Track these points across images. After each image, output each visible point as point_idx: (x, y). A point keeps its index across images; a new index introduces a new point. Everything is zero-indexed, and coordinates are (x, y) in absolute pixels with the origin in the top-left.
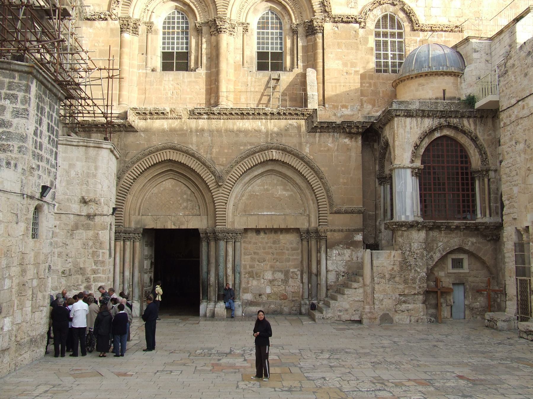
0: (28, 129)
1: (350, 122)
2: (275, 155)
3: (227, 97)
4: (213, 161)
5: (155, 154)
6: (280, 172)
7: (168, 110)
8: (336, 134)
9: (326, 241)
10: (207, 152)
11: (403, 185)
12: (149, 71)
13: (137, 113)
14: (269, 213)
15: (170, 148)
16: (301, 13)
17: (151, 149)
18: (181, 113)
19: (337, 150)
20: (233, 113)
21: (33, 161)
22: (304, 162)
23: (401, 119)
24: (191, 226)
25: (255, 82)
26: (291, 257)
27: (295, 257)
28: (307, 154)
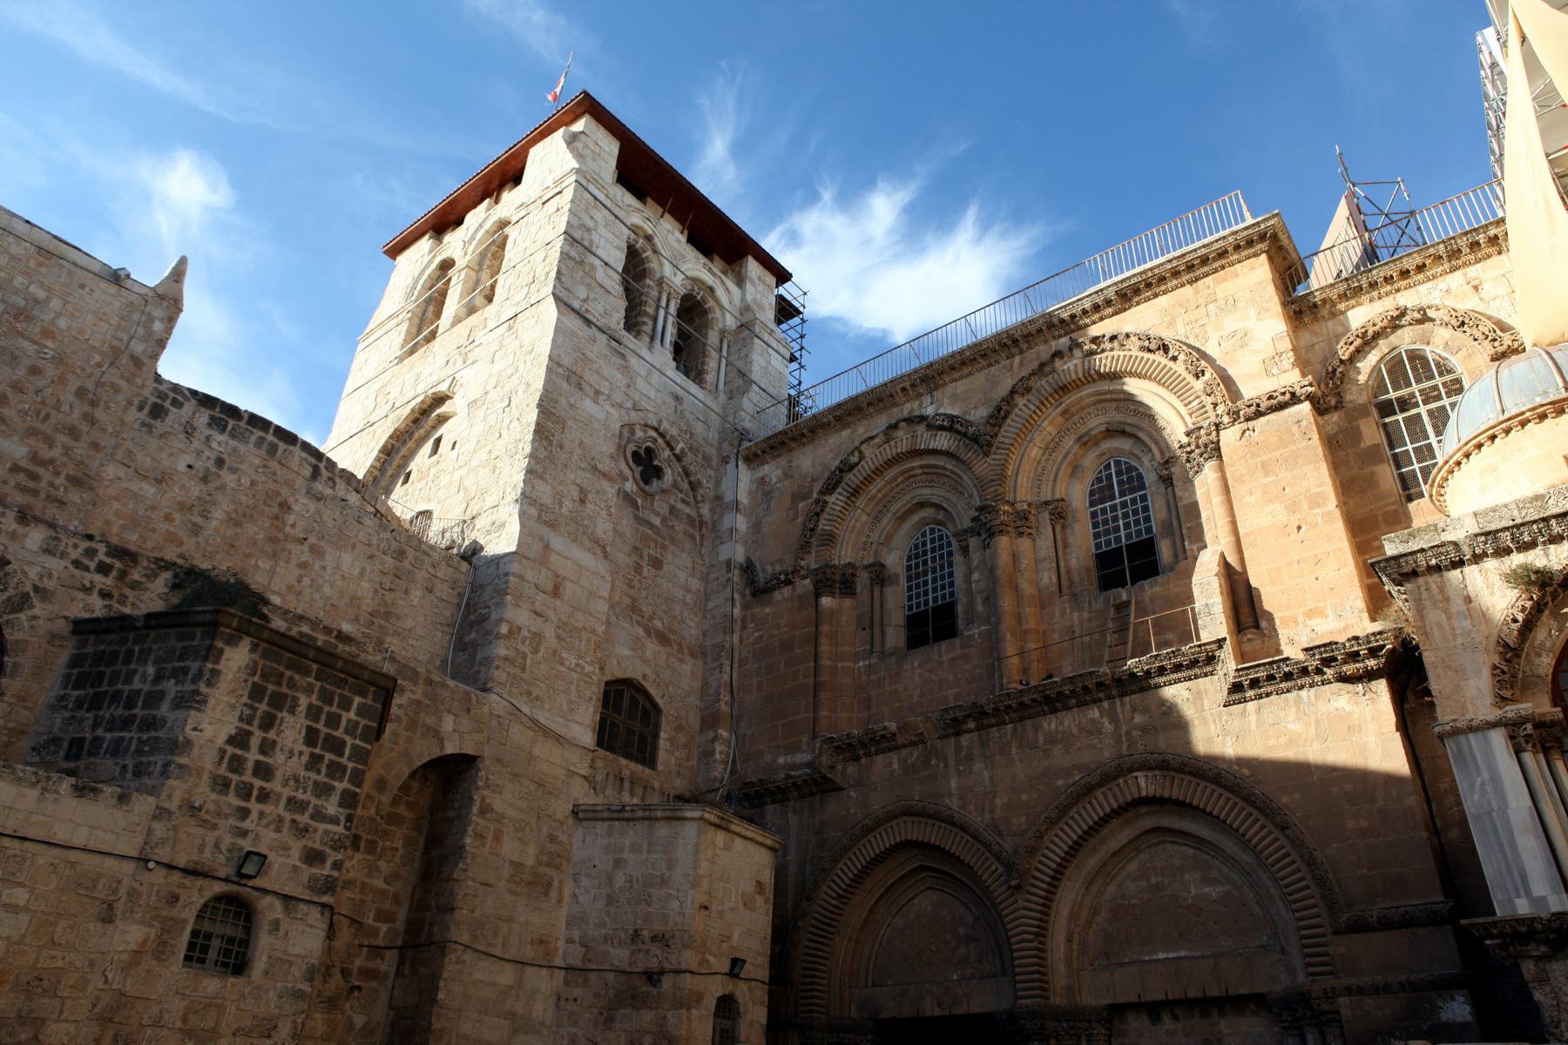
0: (195, 729)
1: (1325, 645)
2: (1144, 784)
9: (1342, 1028)
11: (1489, 789)
13: (838, 747)
14: (1171, 955)
20: (1026, 699)
21: (214, 796)
22: (1225, 787)
23: (1427, 583)
24: (977, 1006)
25: (1090, 620)
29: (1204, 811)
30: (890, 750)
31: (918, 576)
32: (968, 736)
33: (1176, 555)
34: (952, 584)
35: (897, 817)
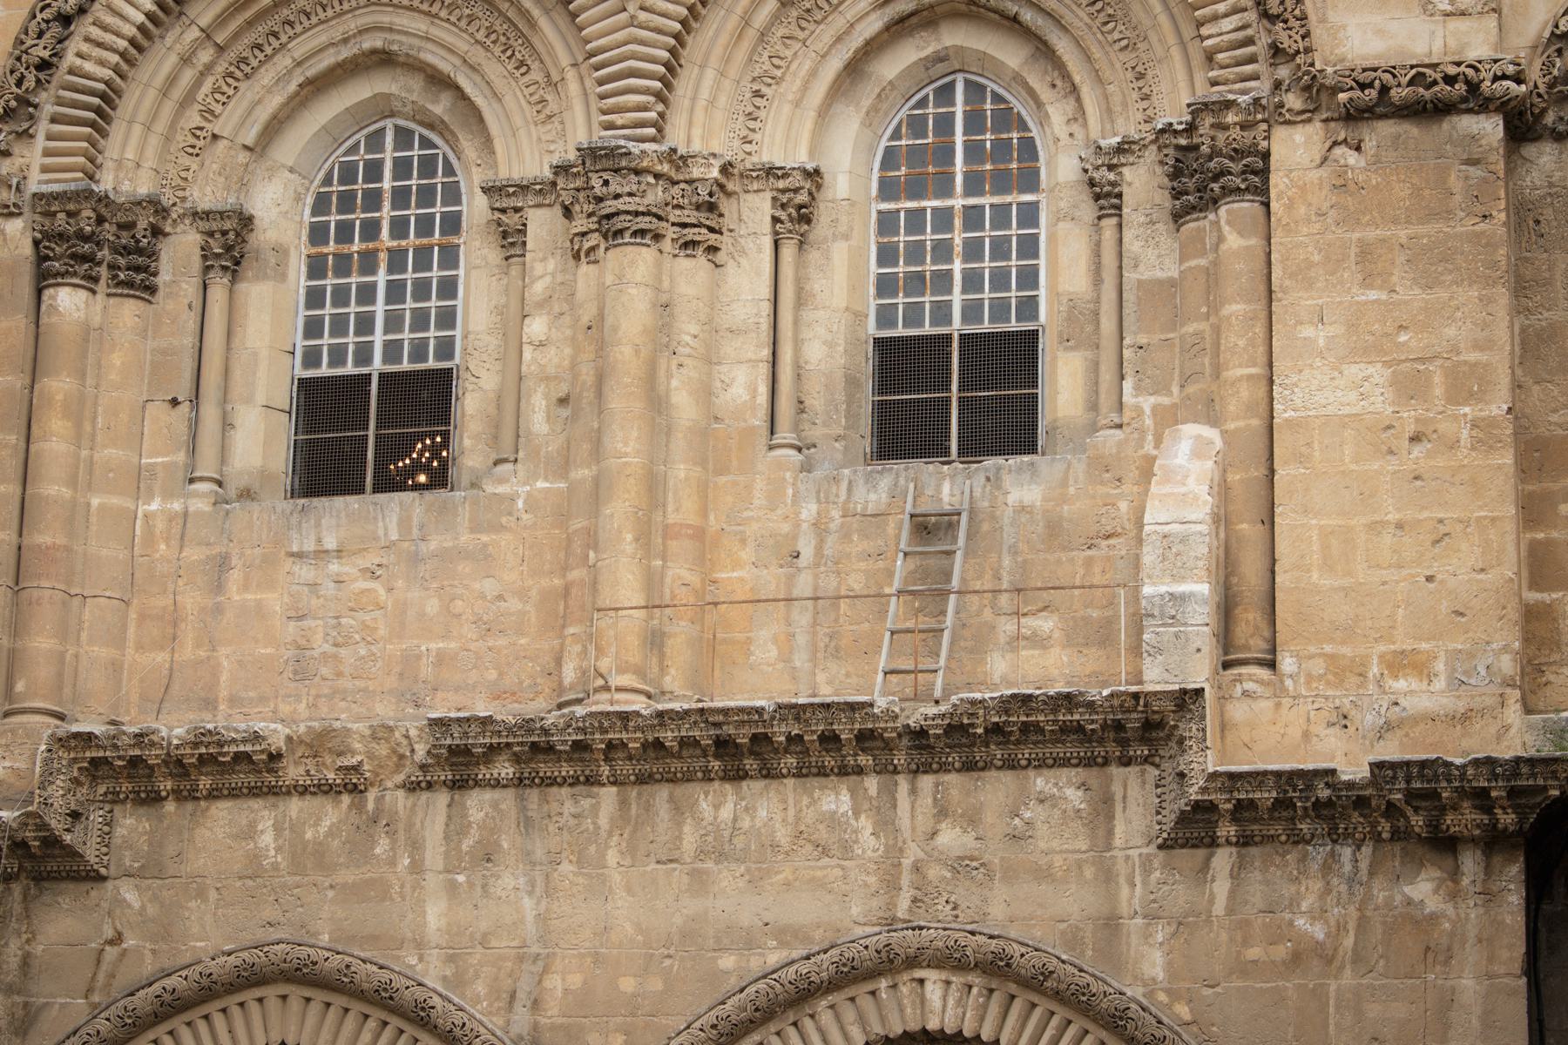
1: (1423, 764)
3: (655, 641)
7: (277, 734)
8: (1346, 852)
10: (513, 996)
12: (200, 500)
13: (94, 762)
16: (1140, 77)
17: (169, 982)
18: (353, 753)
19: (1357, 958)
20: (668, 736)
25: (846, 536)
28: (1150, 994)
30: (255, 792)
31: (343, 265)
32: (488, 795)
33: (1093, 406)
34: (447, 318)
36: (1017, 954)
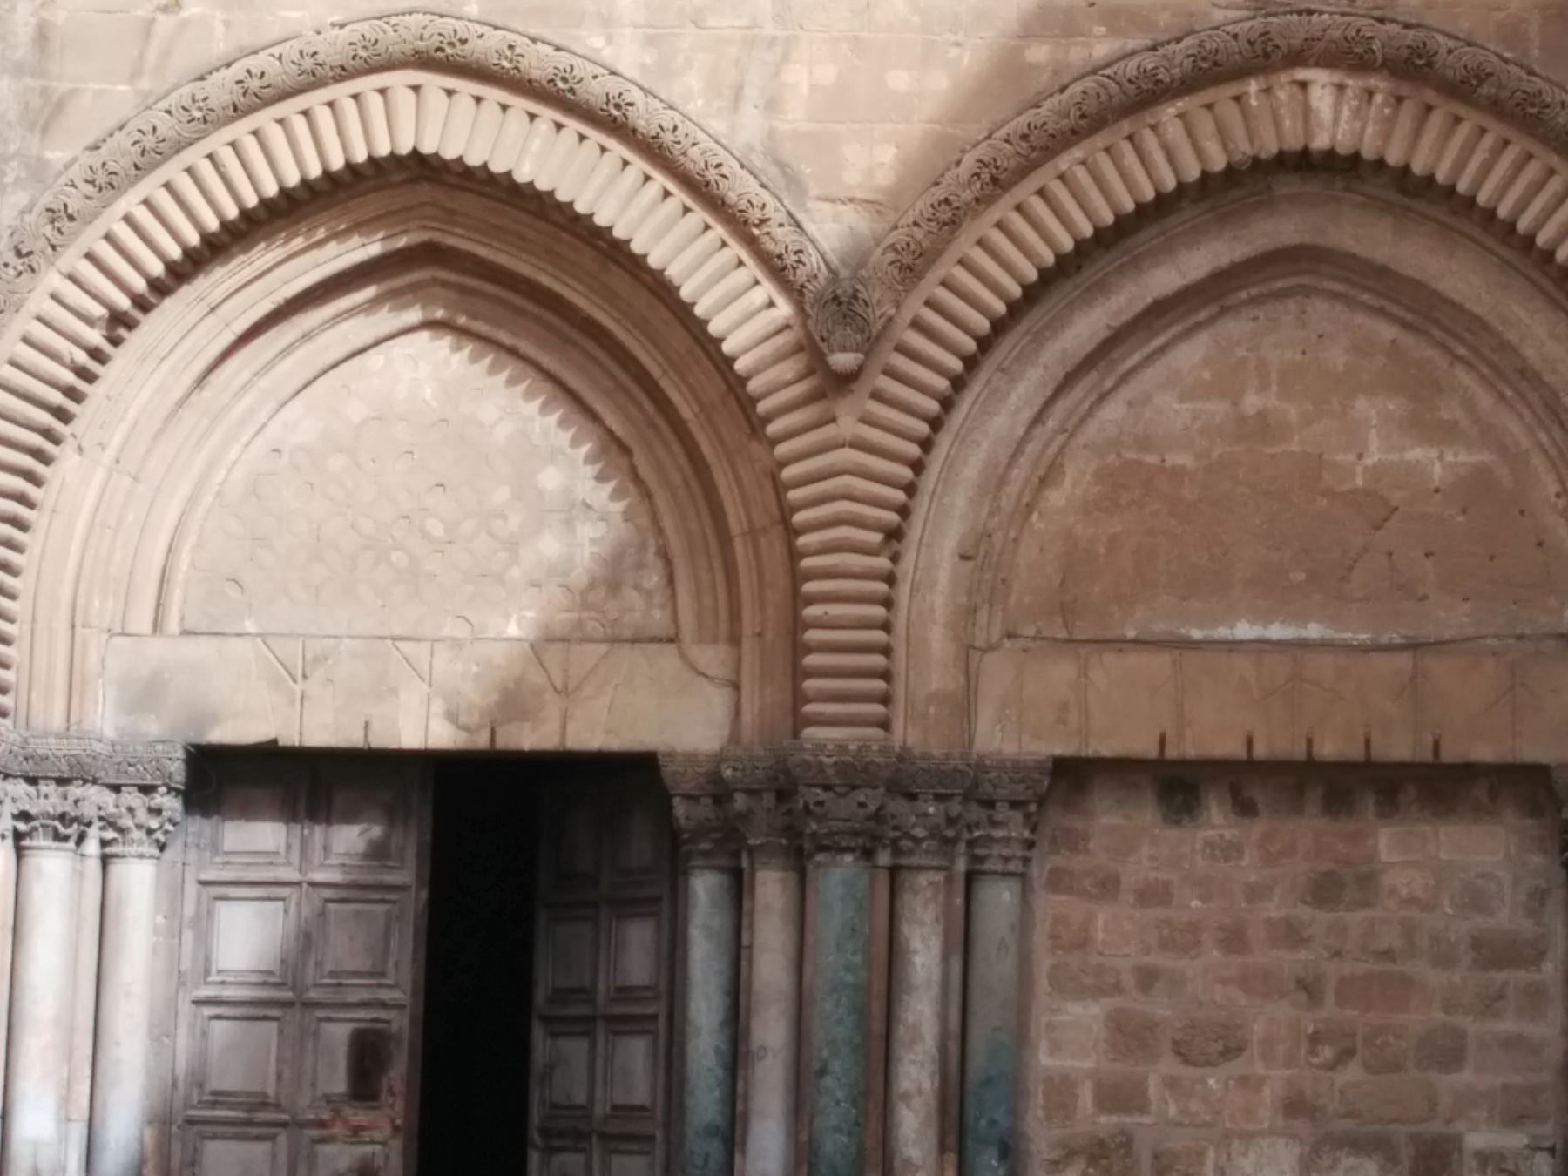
4: (781, 165)
5: (289, 108)
6: (1382, 272)
15: (425, 61)
17: (255, 63)
26: (1471, 1026)
27: (1507, 1025)
29: (1490, 214)
35: (389, 66)
36: (1443, 50)
